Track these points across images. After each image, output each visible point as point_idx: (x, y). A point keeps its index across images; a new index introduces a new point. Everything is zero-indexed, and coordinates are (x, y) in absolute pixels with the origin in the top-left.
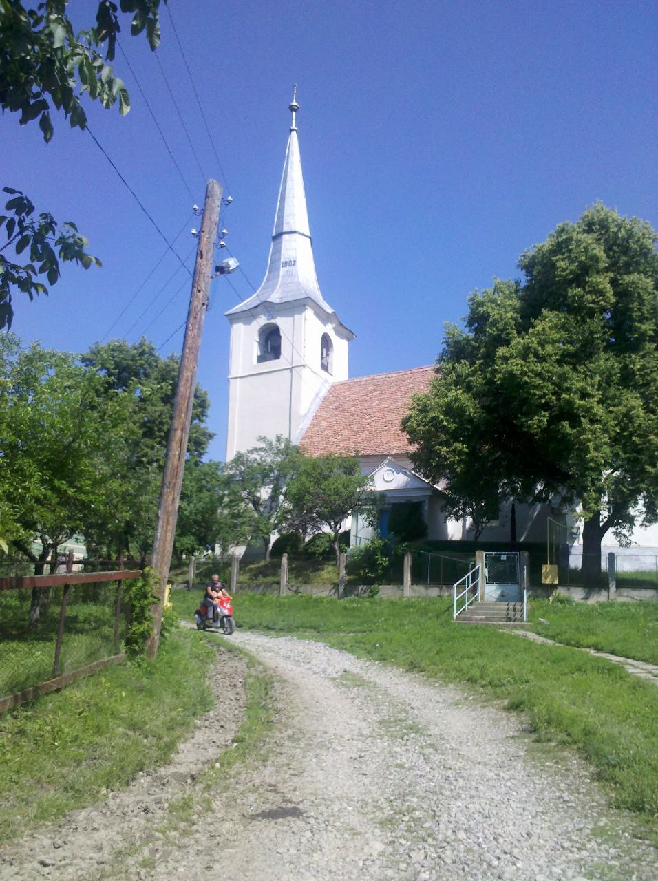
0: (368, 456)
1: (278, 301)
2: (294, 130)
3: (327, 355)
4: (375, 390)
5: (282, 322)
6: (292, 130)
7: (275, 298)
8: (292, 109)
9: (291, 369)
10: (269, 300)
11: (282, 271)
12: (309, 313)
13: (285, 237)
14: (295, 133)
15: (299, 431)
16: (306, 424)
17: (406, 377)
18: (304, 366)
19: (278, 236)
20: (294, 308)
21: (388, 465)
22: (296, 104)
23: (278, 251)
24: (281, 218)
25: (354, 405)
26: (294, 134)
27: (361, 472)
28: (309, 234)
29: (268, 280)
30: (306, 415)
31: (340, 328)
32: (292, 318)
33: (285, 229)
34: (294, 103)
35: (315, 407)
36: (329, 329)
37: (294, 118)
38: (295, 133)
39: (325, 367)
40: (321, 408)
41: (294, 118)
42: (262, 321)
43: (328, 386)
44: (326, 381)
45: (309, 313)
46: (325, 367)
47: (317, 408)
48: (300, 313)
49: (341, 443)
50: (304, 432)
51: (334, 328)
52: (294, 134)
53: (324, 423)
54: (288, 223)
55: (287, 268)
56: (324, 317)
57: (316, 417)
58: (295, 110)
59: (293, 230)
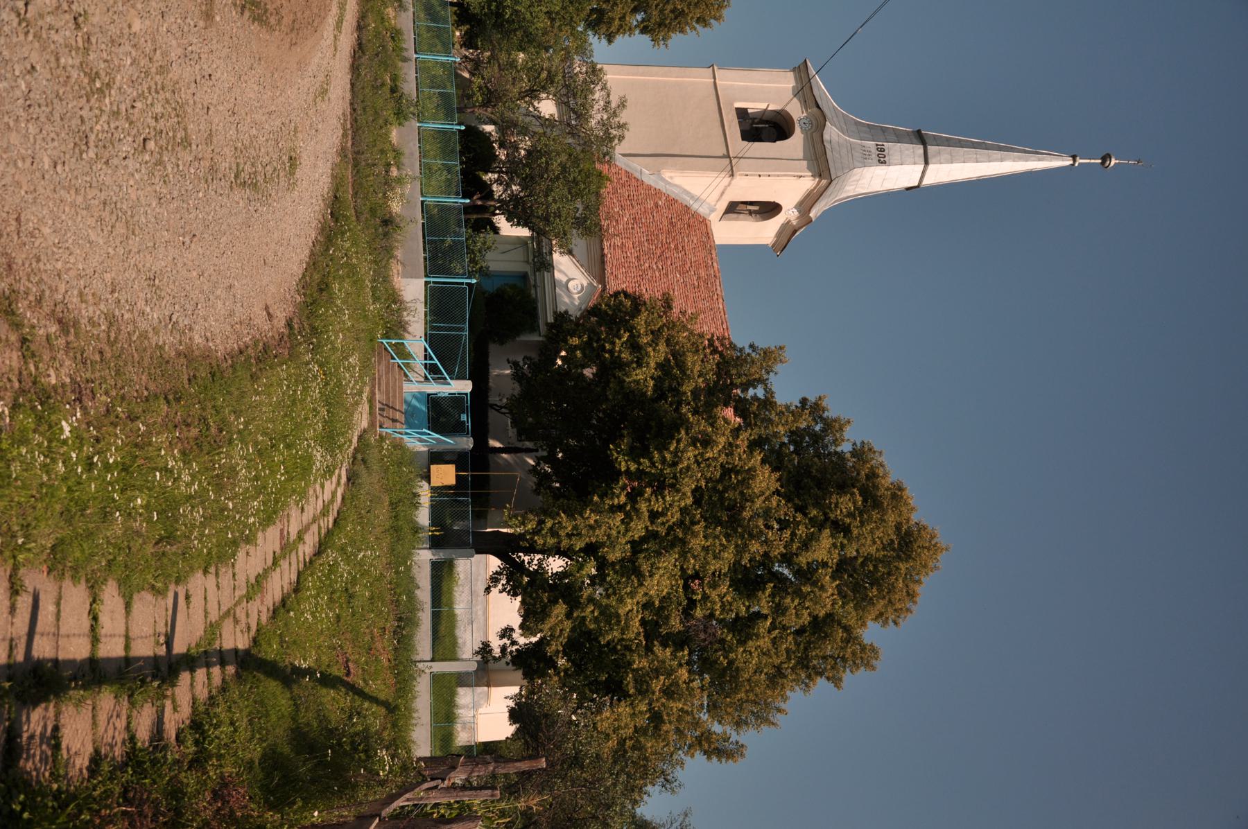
0: (603, 262)
1: (826, 137)
2: (1075, 161)
3: (751, 213)
4: (699, 278)
5: (796, 143)
6: (1074, 157)
7: (832, 133)
8: (1106, 158)
9: (728, 156)
10: (828, 123)
11: (871, 145)
12: (808, 183)
13: (919, 149)
14: (1071, 162)
15: (639, 168)
16: (648, 178)
17: (719, 323)
18: (732, 175)
19: (920, 138)
20: (817, 159)
21: (590, 284)
22: (1112, 163)
23: (899, 138)
24: (948, 143)
25: (676, 248)
26: (1069, 162)
27: (579, 243)
28: (926, 182)
29: (857, 123)
30: (663, 180)
31: (789, 233)
32: (801, 156)
33: (931, 149)
34: (1113, 162)
35: (674, 192)
36: (789, 213)
37: (1093, 161)
38: (1071, 162)
39: (733, 208)
40: (672, 202)
41: (1093, 161)
42: (796, 111)
43: (703, 210)
44: (713, 210)
45: (808, 183)
46: (733, 208)
47: (673, 196)
48: (809, 168)
49: (621, 227)
50: (637, 175)
51: (789, 221)
52: (1069, 162)
53: (650, 204)
54: (939, 153)
55: (874, 149)
56: (805, 205)
57: (659, 193)
58: (1103, 163)
59: (930, 161)
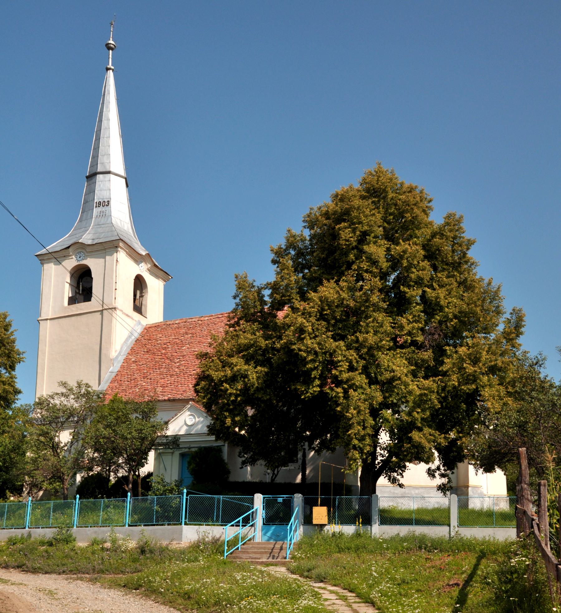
0: (174, 400)
1: (90, 242)
2: (110, 69)
3: (141, 296)
4: (187, 333)
5: (93, 264)
6: (108, 69)
7: (87, 238)
8: (108, 47)
9: (102, 311)
10: (80, 241)
11: (96, 211)
12: (122, 255)
13: (100, 177)
14: (111, 71)
15: (109, 374)
16: (116, 367)
17: (218, 320)
18: (115, 308)
19: (92, 177)
20: (105, 249)
21: (189, 409)
22: (112, 42)
23: (91, 191)
24: (96, 157)
25: (165, 349)
26: (111, 73)
27: (160, 417)
28: (122, 172)
29: (81, 220)
30: (117, 357)
31: (156, 270)
32: (102, 260)
33: (100, 169)
34: (111, 42)
35: (126, 350)
36: (143, 269)
37: (111, 56)
38: (111, 71)
39: (138, 309)
40: (133, 351)
41: (111, 56)
42: (71, 263)
43: (139, 329)
44: (139, 323)
45: (122, 255)
46: (138, 309)
47: (129, 350)
48: (111, 255)
49: (149, 387)
50: (113, 375)
51: (148, 269)
52: (111, 74)
53: (134, 366)
54: (102, 163)
55: (99, 209)
56: (137, 258)
57: (126, 360)
58: (112, 49)
59: (108, 170)
